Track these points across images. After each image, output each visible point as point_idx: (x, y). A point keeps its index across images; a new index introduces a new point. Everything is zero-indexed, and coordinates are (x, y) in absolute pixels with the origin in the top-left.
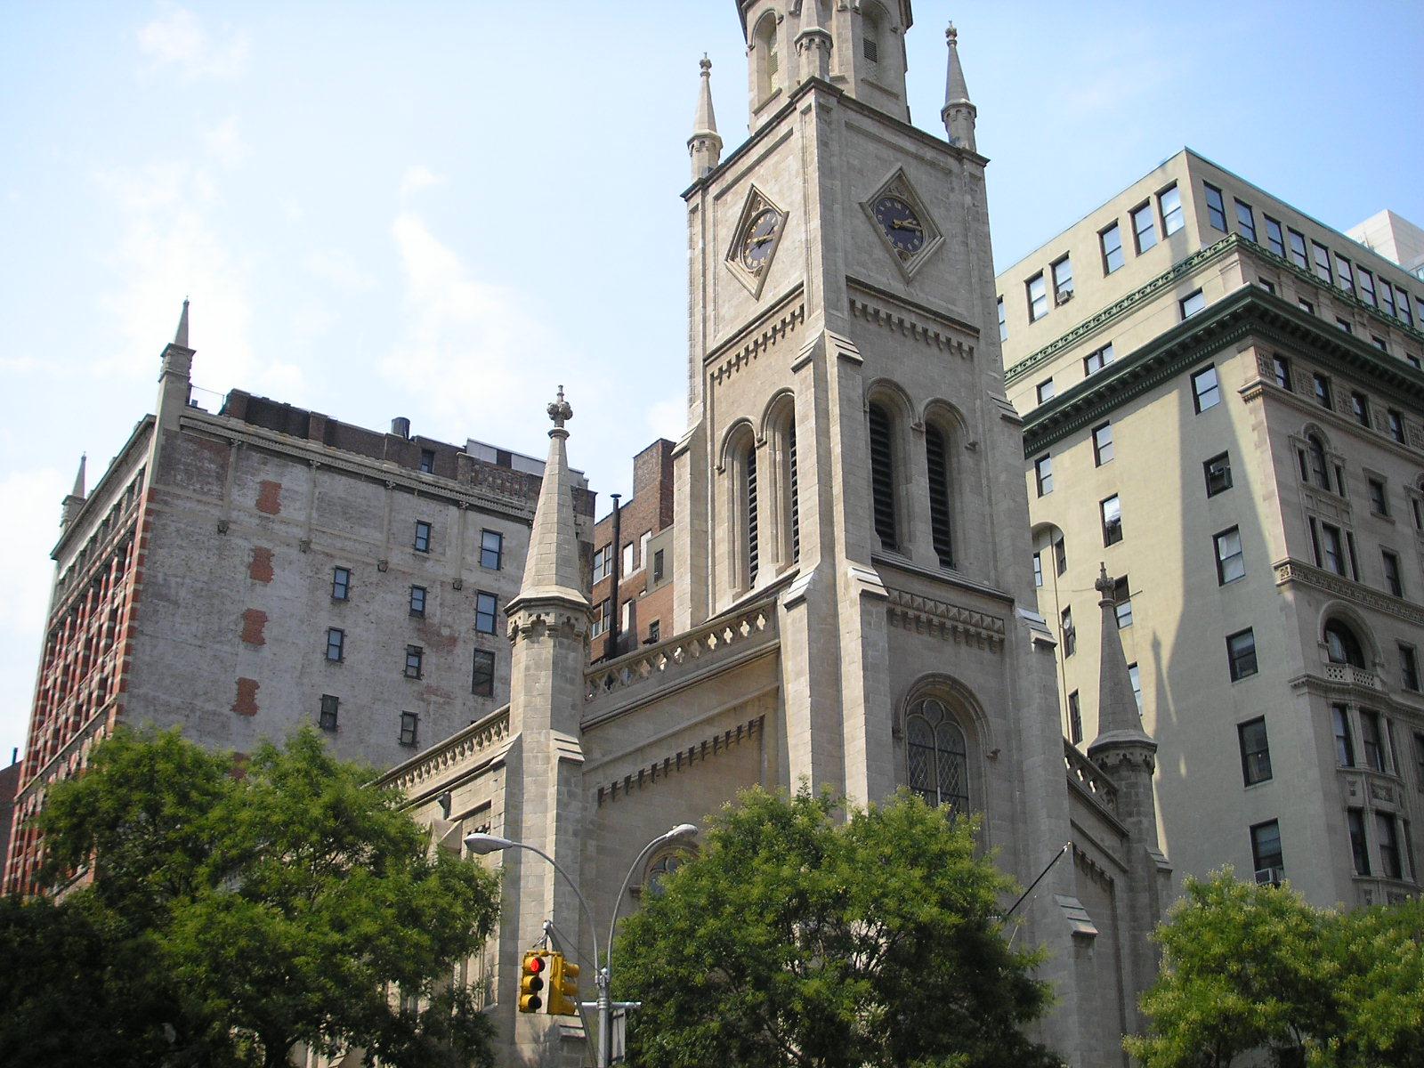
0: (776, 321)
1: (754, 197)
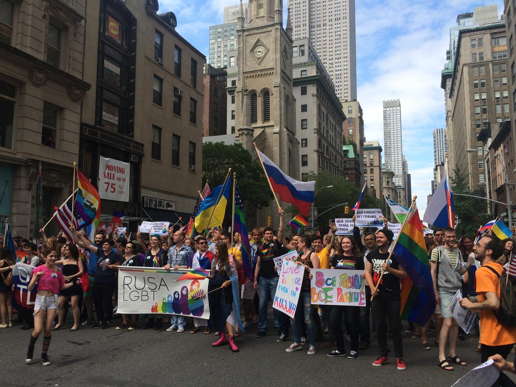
0: (266, 72)
1: (258, 40)
